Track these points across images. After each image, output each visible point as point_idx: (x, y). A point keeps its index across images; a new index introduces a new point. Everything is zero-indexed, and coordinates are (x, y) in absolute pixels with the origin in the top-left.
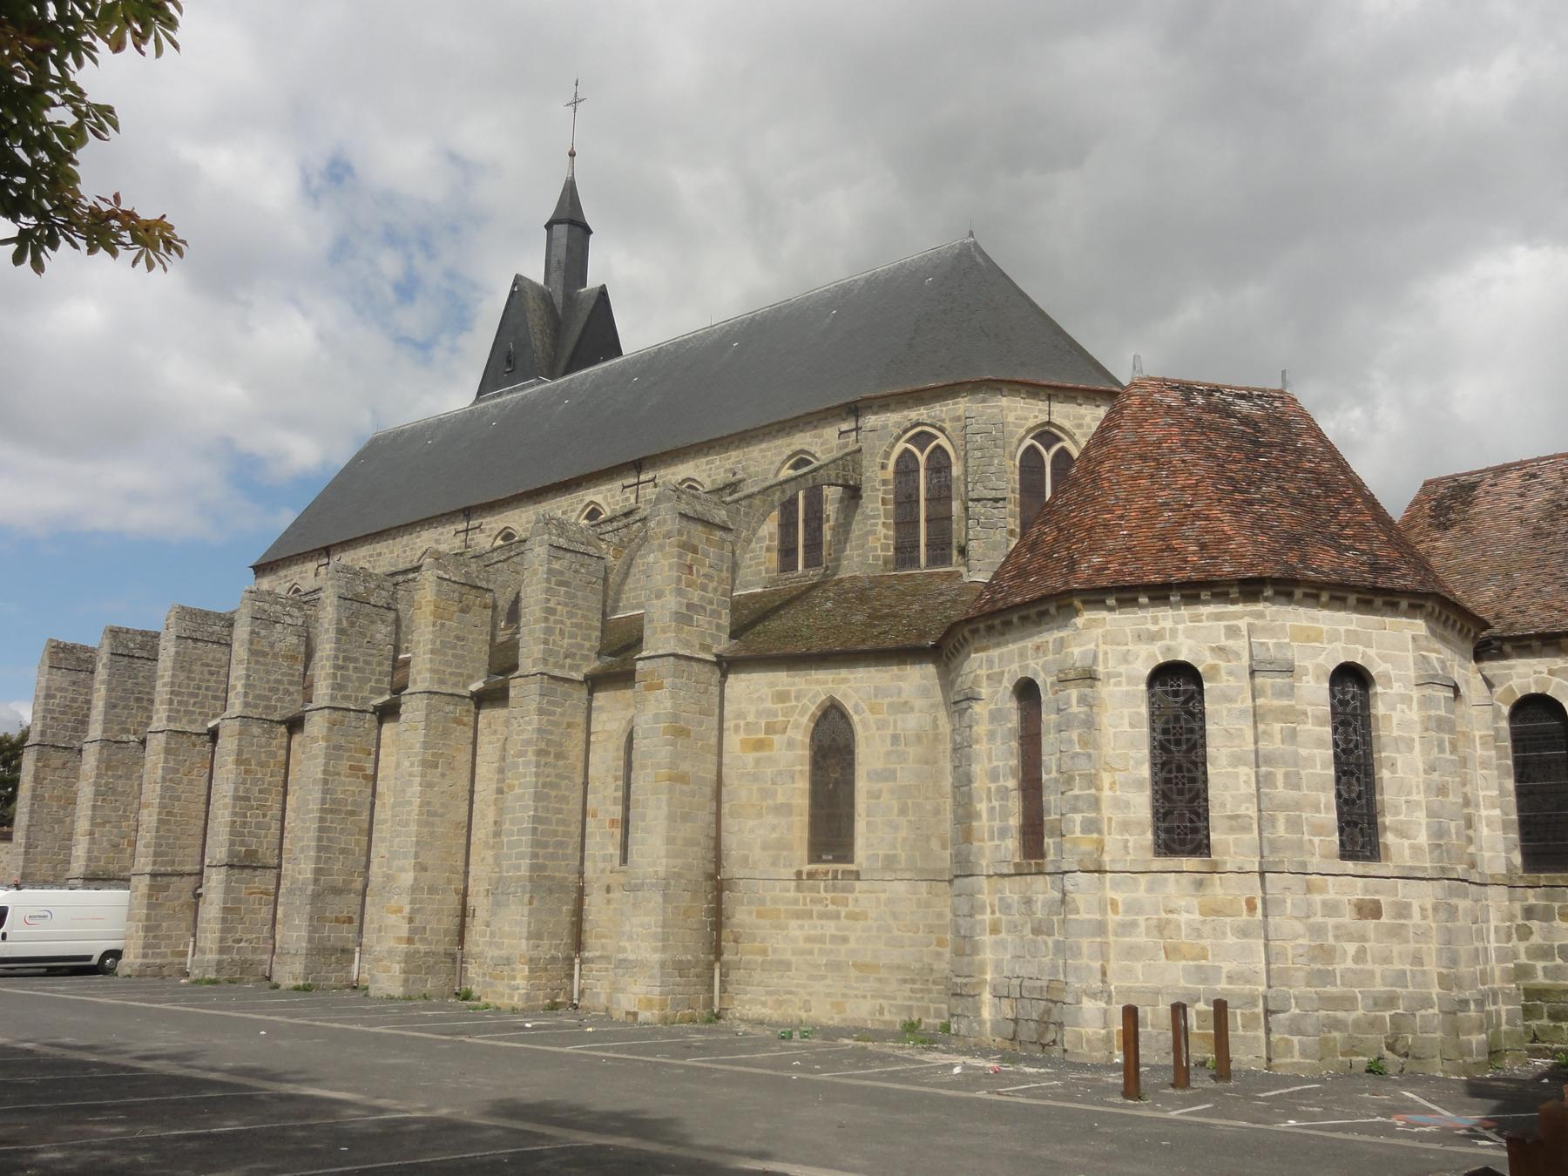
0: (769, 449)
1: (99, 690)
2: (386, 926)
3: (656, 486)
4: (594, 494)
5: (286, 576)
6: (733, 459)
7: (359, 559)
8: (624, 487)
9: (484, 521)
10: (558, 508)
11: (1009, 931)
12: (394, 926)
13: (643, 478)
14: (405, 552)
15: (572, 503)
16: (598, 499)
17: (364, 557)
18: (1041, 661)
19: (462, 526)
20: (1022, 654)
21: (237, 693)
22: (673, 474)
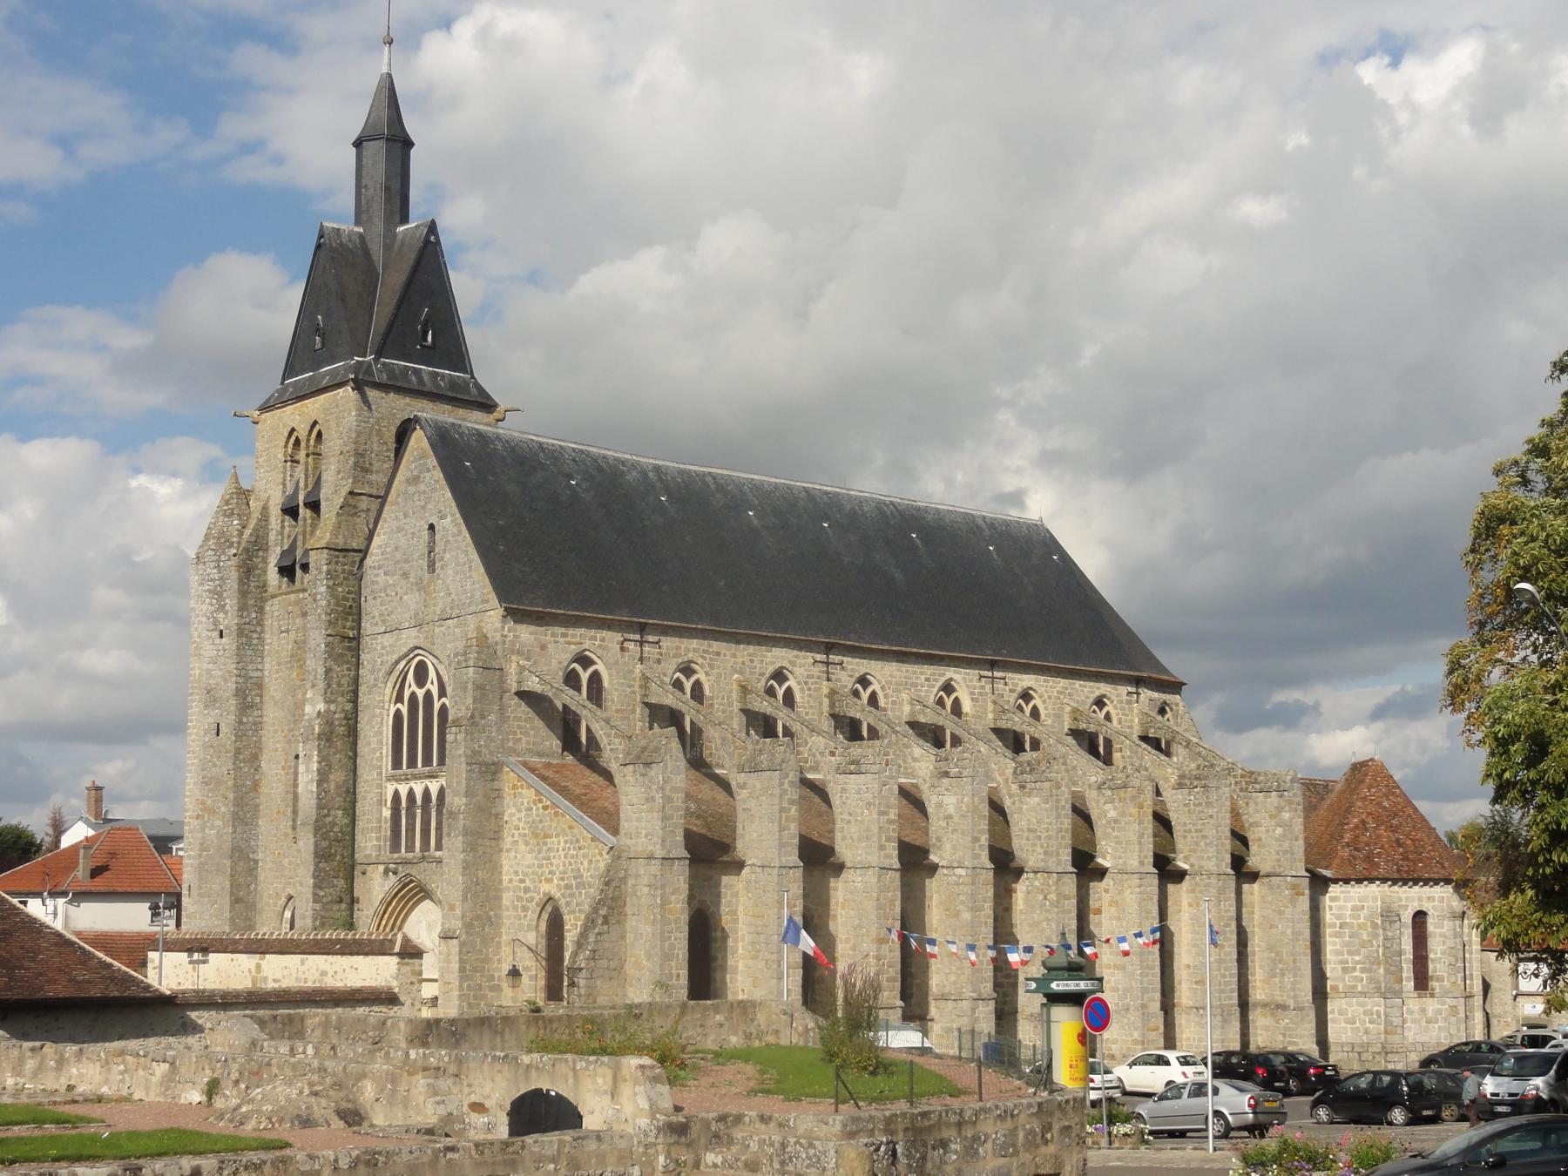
0: (1085, 687)
1: (789, 810)
2: (1148, 1041)
3: (1006, 684)
4: (955, 672)
5: (574, 636)
6: (1061, 685)
7: (687, 650)
8: (981, 677)
9: (846, 659)
10: (922, 673)
11: (1412, 1023)
12: (1153, 1041)
13: (997, 674)
14: (752, 661)
15: (934, 674)
16: (955, 677)
17: (695, 650)
18: (1432, 904)
19: (819, 657)
20: (1420, 899)
21: (981, 846)
22: (1019, 680)
